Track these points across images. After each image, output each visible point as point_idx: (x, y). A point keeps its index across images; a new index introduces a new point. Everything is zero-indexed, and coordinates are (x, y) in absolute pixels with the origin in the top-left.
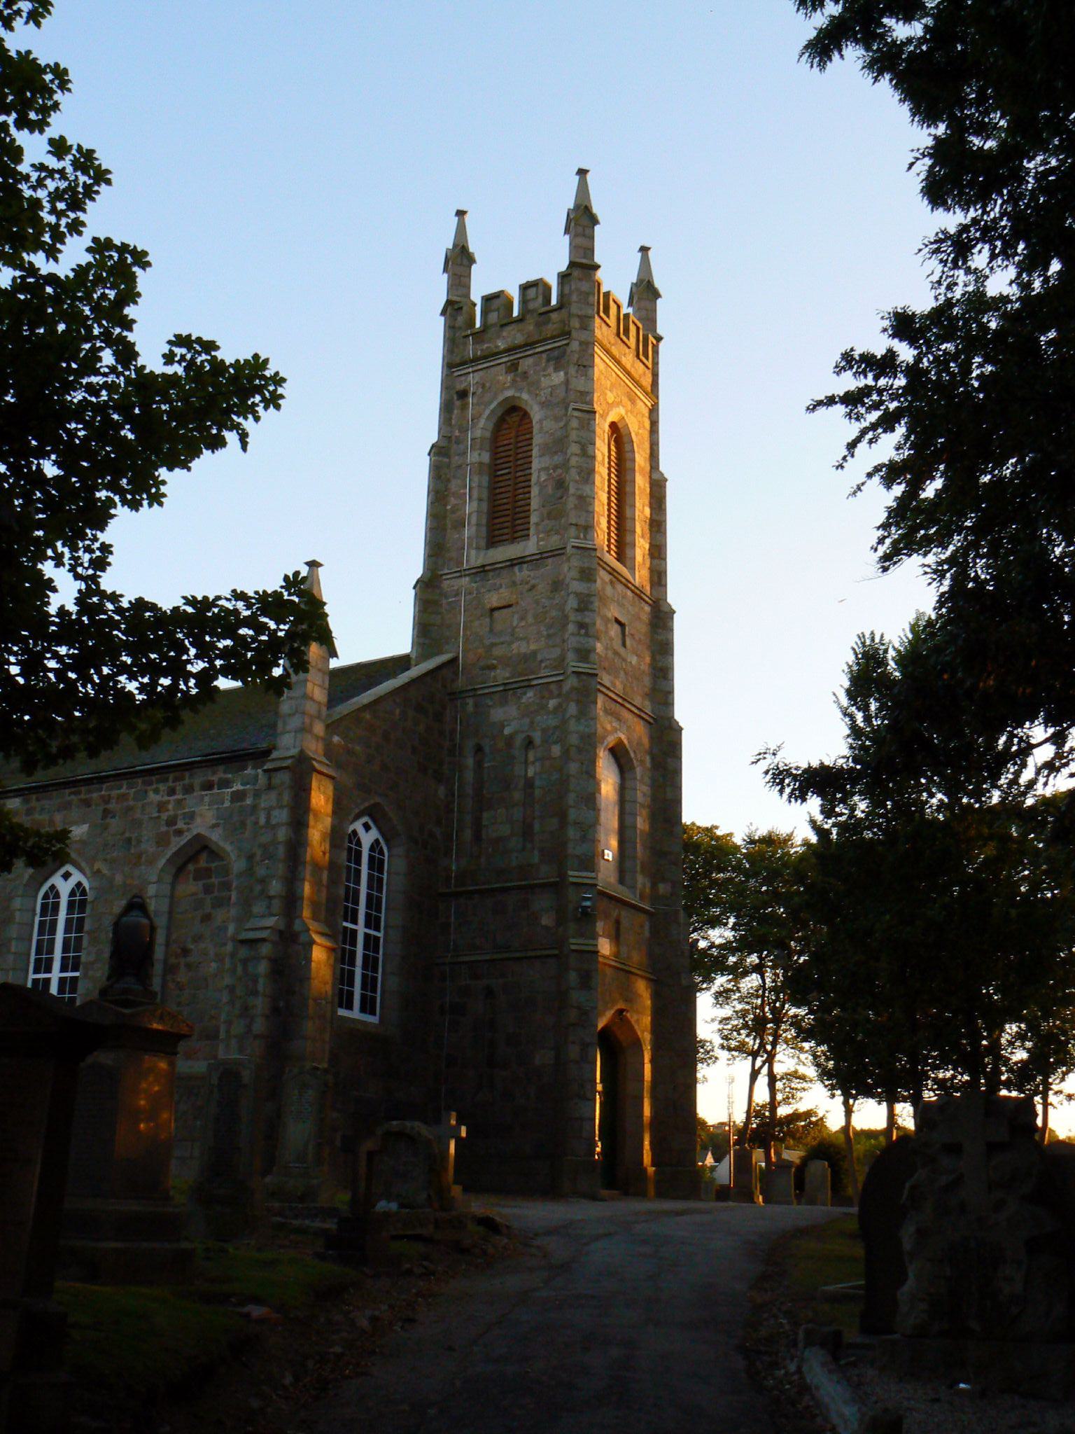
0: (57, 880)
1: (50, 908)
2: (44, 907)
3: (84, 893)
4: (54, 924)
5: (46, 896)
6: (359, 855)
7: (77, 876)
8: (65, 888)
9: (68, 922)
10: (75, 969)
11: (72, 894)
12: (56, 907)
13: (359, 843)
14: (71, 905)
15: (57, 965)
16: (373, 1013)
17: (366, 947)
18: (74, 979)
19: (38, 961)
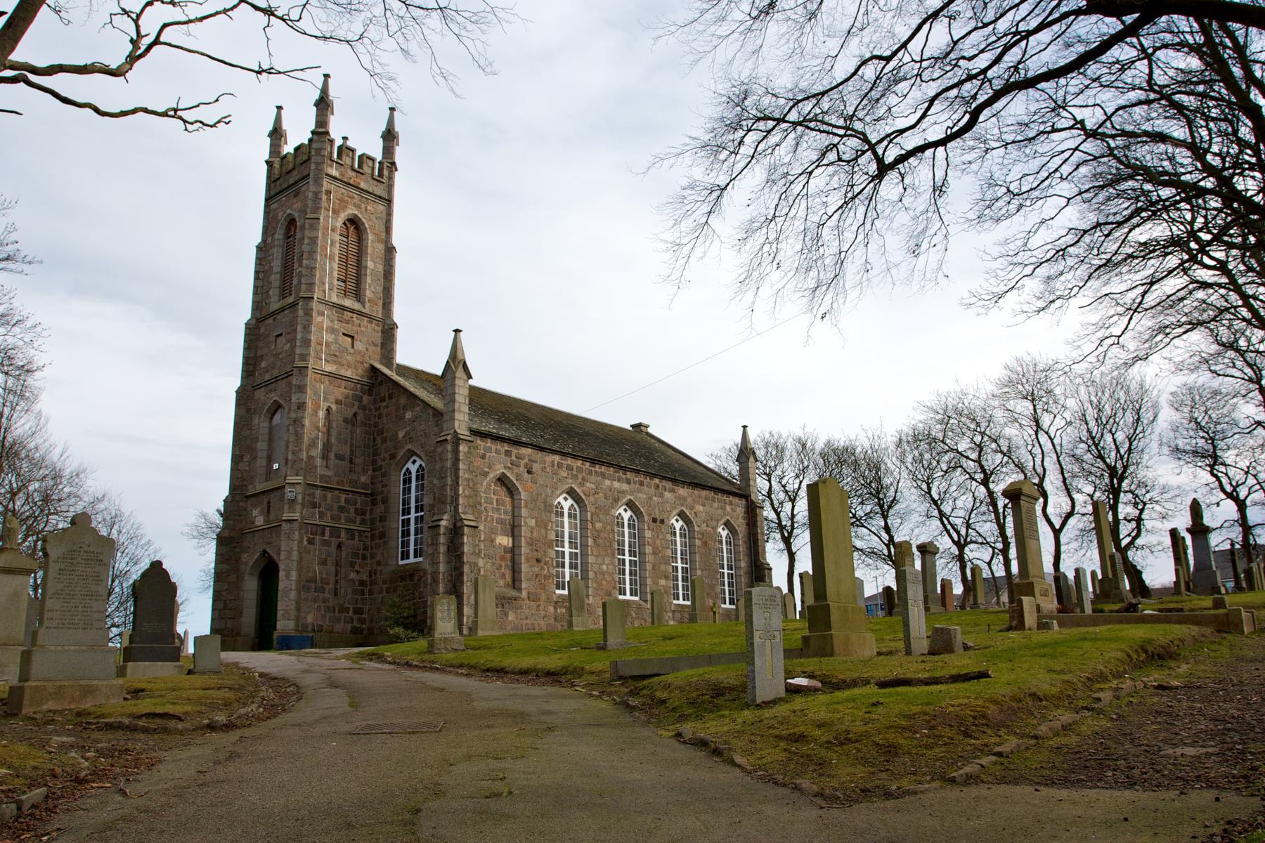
0: (409, 465)
1: (407, 480)
2: (405, 480)
3: (423, 470)
4: (410, 488)
5: (405, 474)
6: (623, 523)
7: (419, 462)
8: (414, 469)
9: (417, 486)
10: (422, 511)
11: (418, 471)
12: (410, 479)
13: (622, 519)
14: (417, 477)
15: (413, 510)
16: (636, 595)
17: (630, 566)
18: (422, 516)
19: (404, 510)
